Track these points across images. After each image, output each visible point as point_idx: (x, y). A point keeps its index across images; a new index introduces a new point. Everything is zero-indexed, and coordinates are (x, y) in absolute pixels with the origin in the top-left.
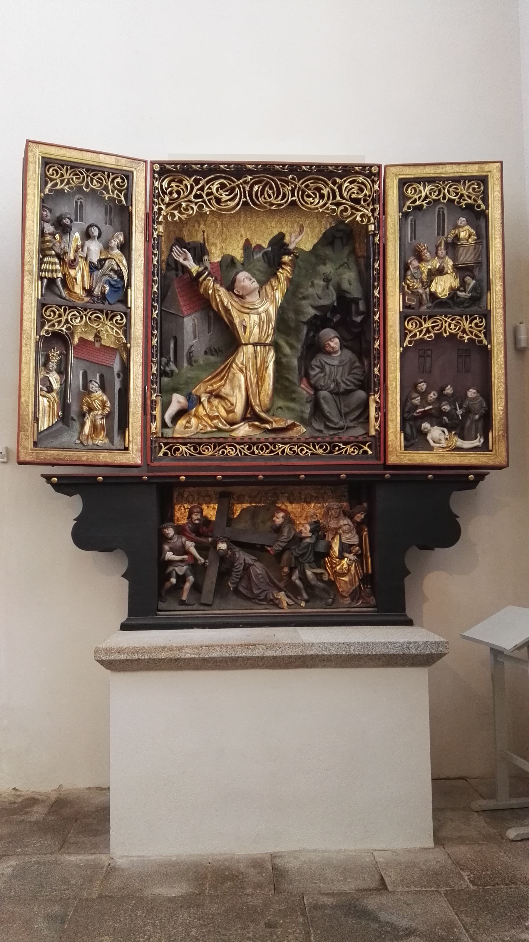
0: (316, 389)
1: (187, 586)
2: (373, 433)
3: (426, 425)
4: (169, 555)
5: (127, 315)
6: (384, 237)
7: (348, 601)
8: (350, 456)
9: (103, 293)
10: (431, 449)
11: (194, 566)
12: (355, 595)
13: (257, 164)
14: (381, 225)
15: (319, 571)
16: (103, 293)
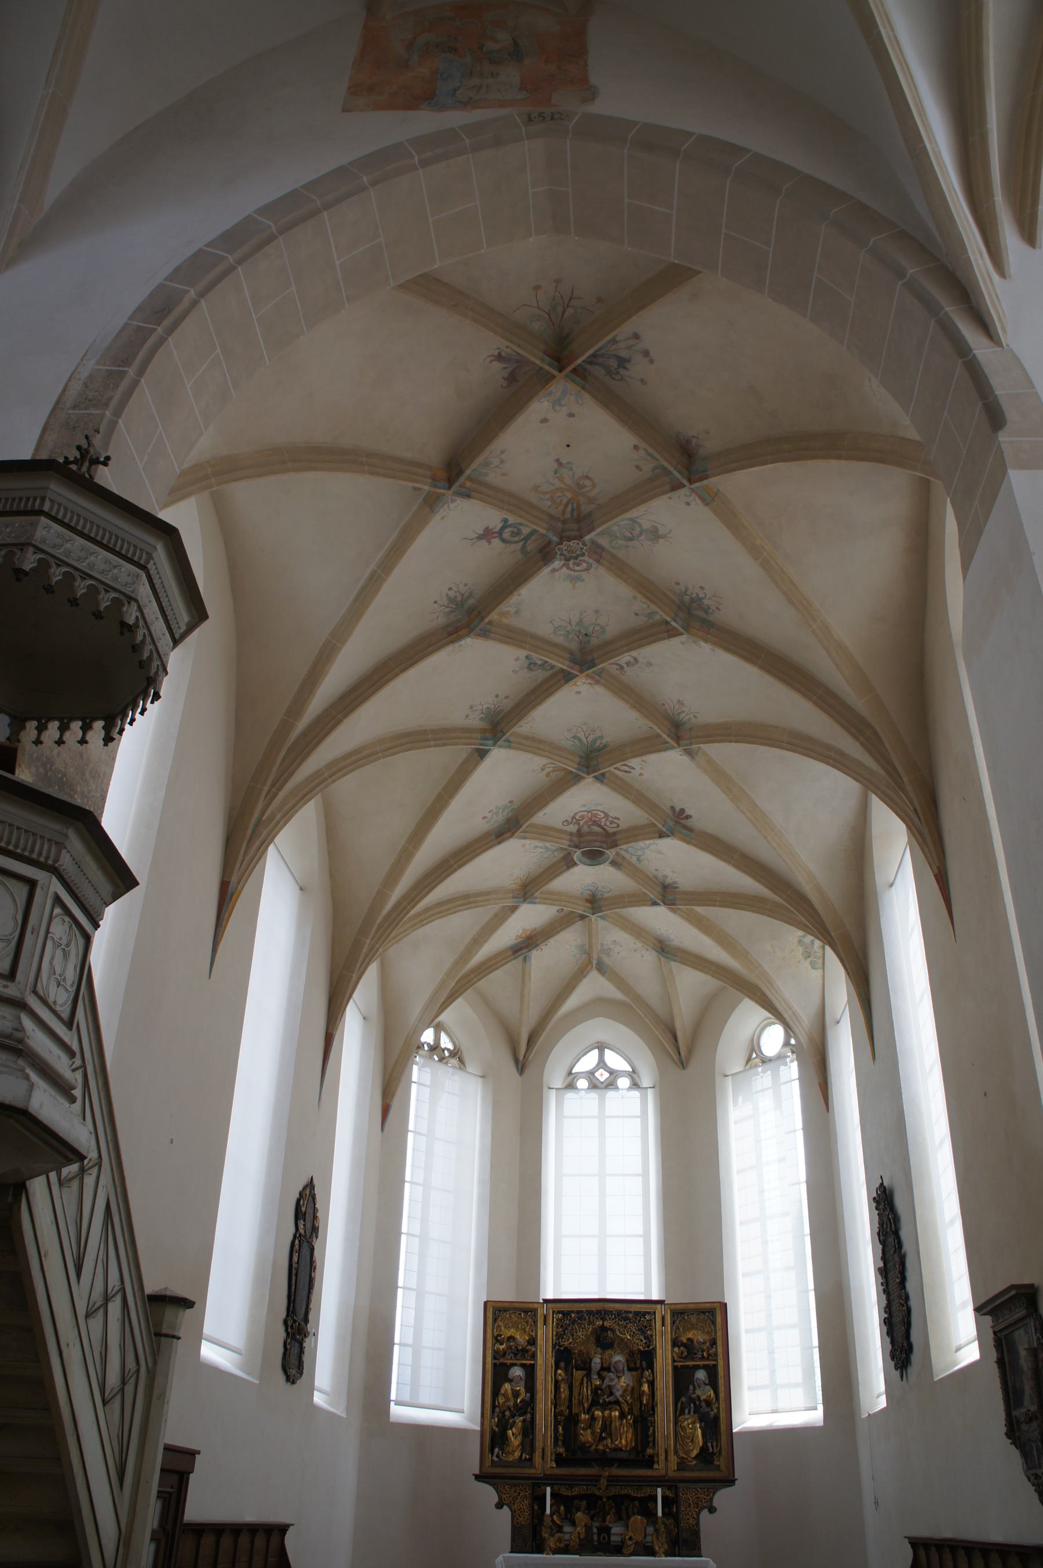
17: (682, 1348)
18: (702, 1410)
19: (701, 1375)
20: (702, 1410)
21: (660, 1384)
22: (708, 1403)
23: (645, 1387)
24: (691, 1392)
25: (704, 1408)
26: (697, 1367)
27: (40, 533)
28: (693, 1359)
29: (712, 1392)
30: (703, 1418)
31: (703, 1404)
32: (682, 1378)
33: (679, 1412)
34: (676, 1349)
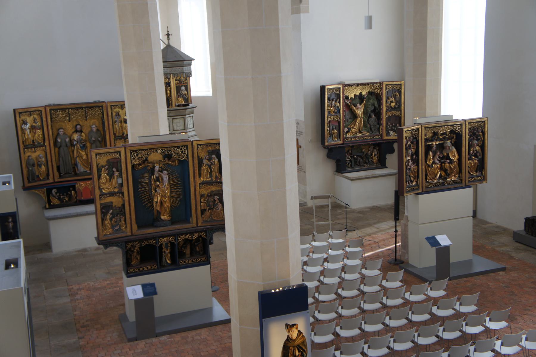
0: (370, 125)
1: (350, 164)
2: (380, 133)
3: (390, 131)
4: (347, 159)
5: (340, 115)
6: (383, 97)
7: (376, 165)
8: (377, 138)
9: (336, 112)
10: (391, 136)
11: (350, 161)
12: (377, 163)
13: (361, 83)
14: (382, 93)
15: (371, 160)
16: (336, 112)
17: (178, 81)
18: (184, 97)
19: (183, 88)
20: (184, 97)
21: (172, 90)
22: (185, 95)
23: (169, 92)
24: (181, 92)
25: (185, 96)
26: (182, 86)
27: (184, 69)
28: (181, 84)
29: (186, 92)
30: (184, 99)
31: (184, 95)
32: (178, 89)
33: (178, 97)
34: (176, 82)
